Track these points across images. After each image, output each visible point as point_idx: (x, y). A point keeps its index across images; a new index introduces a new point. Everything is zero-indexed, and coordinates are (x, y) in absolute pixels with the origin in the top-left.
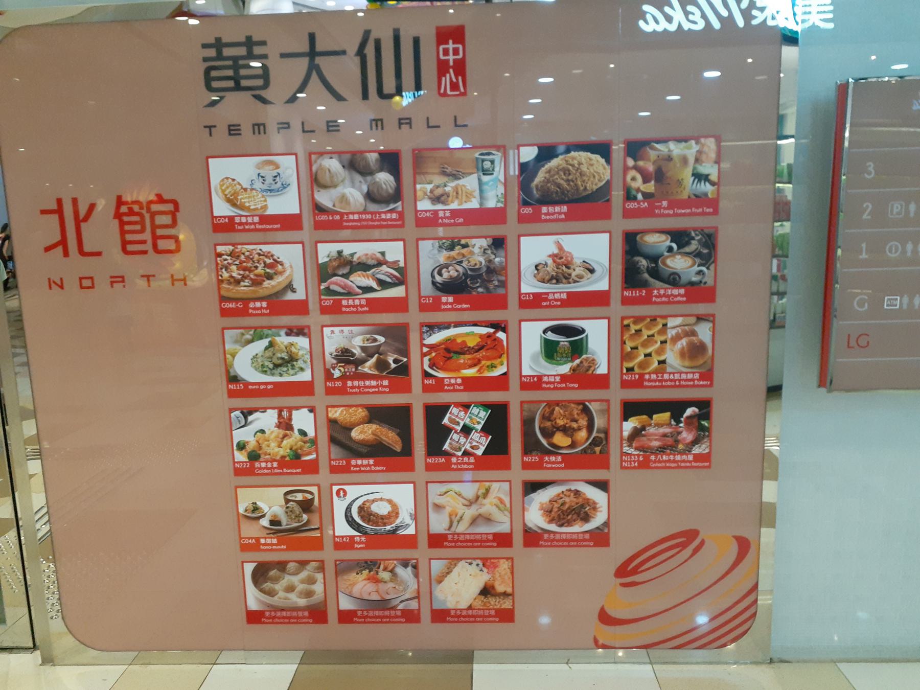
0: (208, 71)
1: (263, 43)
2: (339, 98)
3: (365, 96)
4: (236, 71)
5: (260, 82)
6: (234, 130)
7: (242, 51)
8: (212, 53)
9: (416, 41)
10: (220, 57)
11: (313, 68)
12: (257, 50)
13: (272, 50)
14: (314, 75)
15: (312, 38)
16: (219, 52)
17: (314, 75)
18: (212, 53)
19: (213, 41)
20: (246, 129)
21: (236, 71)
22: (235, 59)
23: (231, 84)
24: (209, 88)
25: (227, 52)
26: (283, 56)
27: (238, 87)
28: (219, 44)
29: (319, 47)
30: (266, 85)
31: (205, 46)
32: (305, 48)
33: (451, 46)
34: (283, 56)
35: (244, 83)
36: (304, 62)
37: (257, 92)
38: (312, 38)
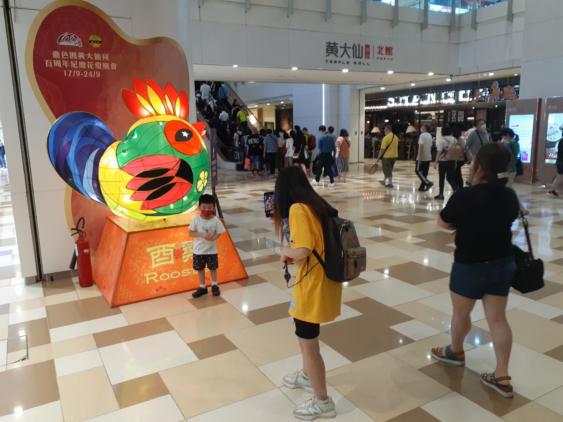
0: (327, 49)
1: (337, 44)
2: (349, 57)
3: (354, 57)
4: (332, 49)
5: (336, 52)
6: (331, 62)
7: (333, 45)
8: (328, 45)
9: (362, 47)
10: (329, 46)
11: (345, 51)
12: (336, 45)
13: (339, 46)
14: (345, 53)
15: (345, 44)
16: (329, 45)
17: (345, 53)
18: (328, 45)
19: (328, 42)
20: (333, 62)
21: (332, 49)
22: (332, 47)
23: (331, 52)
24: (327, 52)
25: (331, 45)
26: (340, 47)
27: (332, 53)
28: (329, 43)
29: (347, 46)
30: (337, 53)
31: (327, 43)
32: (344, 46)
33: (368, 49)
34: (340, 47)
35: (334, 52)
36: (343, 49)
37: (336, 54)
38: (345, 44)
